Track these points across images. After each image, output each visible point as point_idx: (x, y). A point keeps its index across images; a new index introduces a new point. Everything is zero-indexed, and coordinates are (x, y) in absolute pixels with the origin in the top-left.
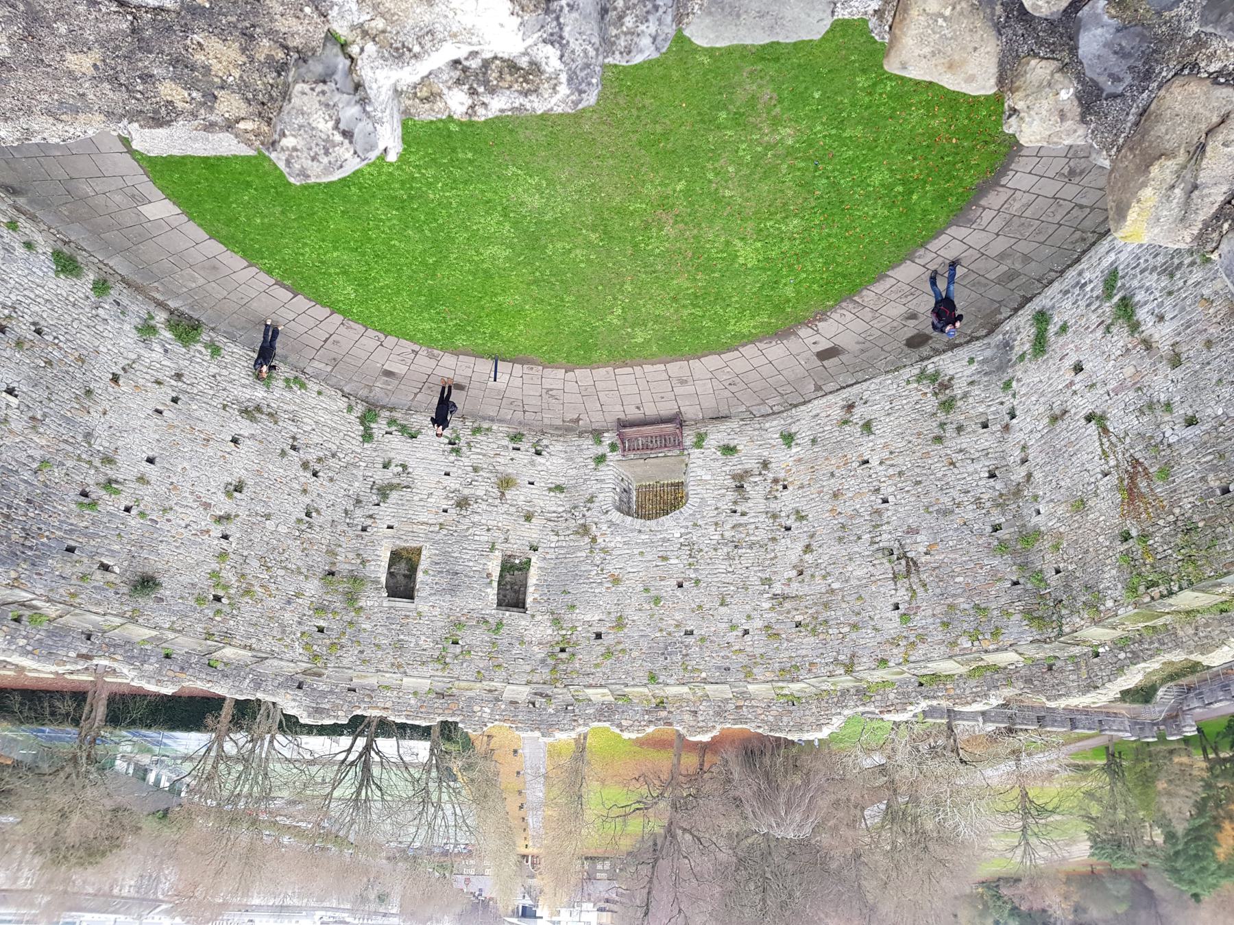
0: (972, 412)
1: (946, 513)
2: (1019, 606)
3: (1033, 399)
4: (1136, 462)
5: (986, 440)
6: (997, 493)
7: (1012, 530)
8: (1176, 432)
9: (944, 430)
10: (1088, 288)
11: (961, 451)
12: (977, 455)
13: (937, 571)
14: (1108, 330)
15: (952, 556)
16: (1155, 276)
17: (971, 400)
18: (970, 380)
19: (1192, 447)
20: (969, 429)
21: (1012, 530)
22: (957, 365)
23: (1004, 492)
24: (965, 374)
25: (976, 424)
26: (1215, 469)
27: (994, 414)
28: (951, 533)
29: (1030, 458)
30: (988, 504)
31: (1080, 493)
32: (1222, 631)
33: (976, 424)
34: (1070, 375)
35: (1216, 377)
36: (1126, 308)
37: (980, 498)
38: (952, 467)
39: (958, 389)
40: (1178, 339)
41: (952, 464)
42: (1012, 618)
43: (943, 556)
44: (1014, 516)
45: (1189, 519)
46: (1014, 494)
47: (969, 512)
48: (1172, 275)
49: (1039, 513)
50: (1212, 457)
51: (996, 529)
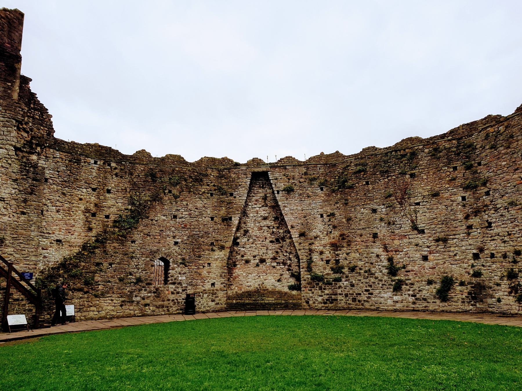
0: (499, 266)
1: (512, 204)
2: (477, 152)
3: (458, 257)
4: (401, 203)
5: (491, 246)
6: (487, 212)
7: (480, 192)
8: (380, 209)
9: (514, 258)
10: (411, 292)
11: (505, 242)
12: (496, 238)
13: (516, 167)
14: (404, 267)
15: (508, 177)
16: (376, 275)
17: (499, 274)
18: (499, 288)
19: (375, 201)
20: (500, 255)
21: (480, 192)
22: (508, 302)
23: (483, 213)
24: (501, 293)
25: (496, 257)
26: (368, 191)
27: (487, 260)
28: (509, 191)
29: (464, 227)
30: (491, 207)
31: (433, 199)
32: (402, 145)
33: (496, 257)
34: (431, 257)
35: (362, 222)
36: (393, 271)
37: (495, 211)
38: (510, 232)
39: (505, 284)
40: (372, 244)
41: (509, 235)
42: (481, 145)
43: (513, 177)
44: (479, 198)
45: (382, 176)
46: (479, 211)
47: (500, 203)
48: (369, 270)
49: (464, 198)
50: (369, 195)
51: (487, 194)
